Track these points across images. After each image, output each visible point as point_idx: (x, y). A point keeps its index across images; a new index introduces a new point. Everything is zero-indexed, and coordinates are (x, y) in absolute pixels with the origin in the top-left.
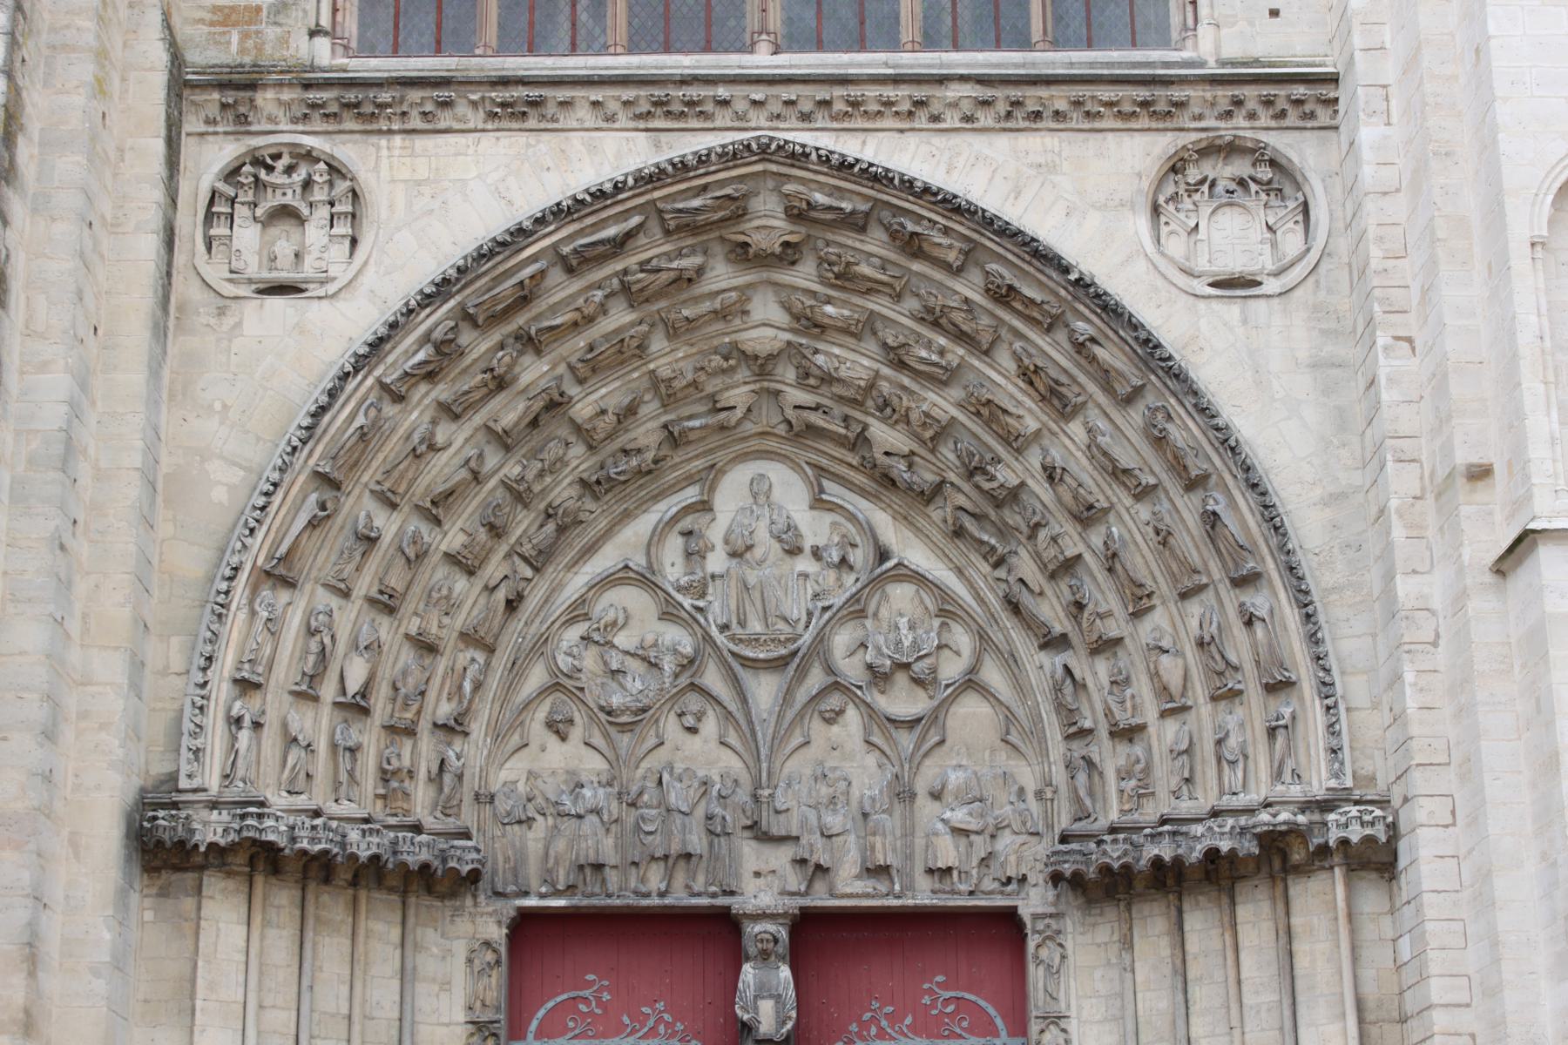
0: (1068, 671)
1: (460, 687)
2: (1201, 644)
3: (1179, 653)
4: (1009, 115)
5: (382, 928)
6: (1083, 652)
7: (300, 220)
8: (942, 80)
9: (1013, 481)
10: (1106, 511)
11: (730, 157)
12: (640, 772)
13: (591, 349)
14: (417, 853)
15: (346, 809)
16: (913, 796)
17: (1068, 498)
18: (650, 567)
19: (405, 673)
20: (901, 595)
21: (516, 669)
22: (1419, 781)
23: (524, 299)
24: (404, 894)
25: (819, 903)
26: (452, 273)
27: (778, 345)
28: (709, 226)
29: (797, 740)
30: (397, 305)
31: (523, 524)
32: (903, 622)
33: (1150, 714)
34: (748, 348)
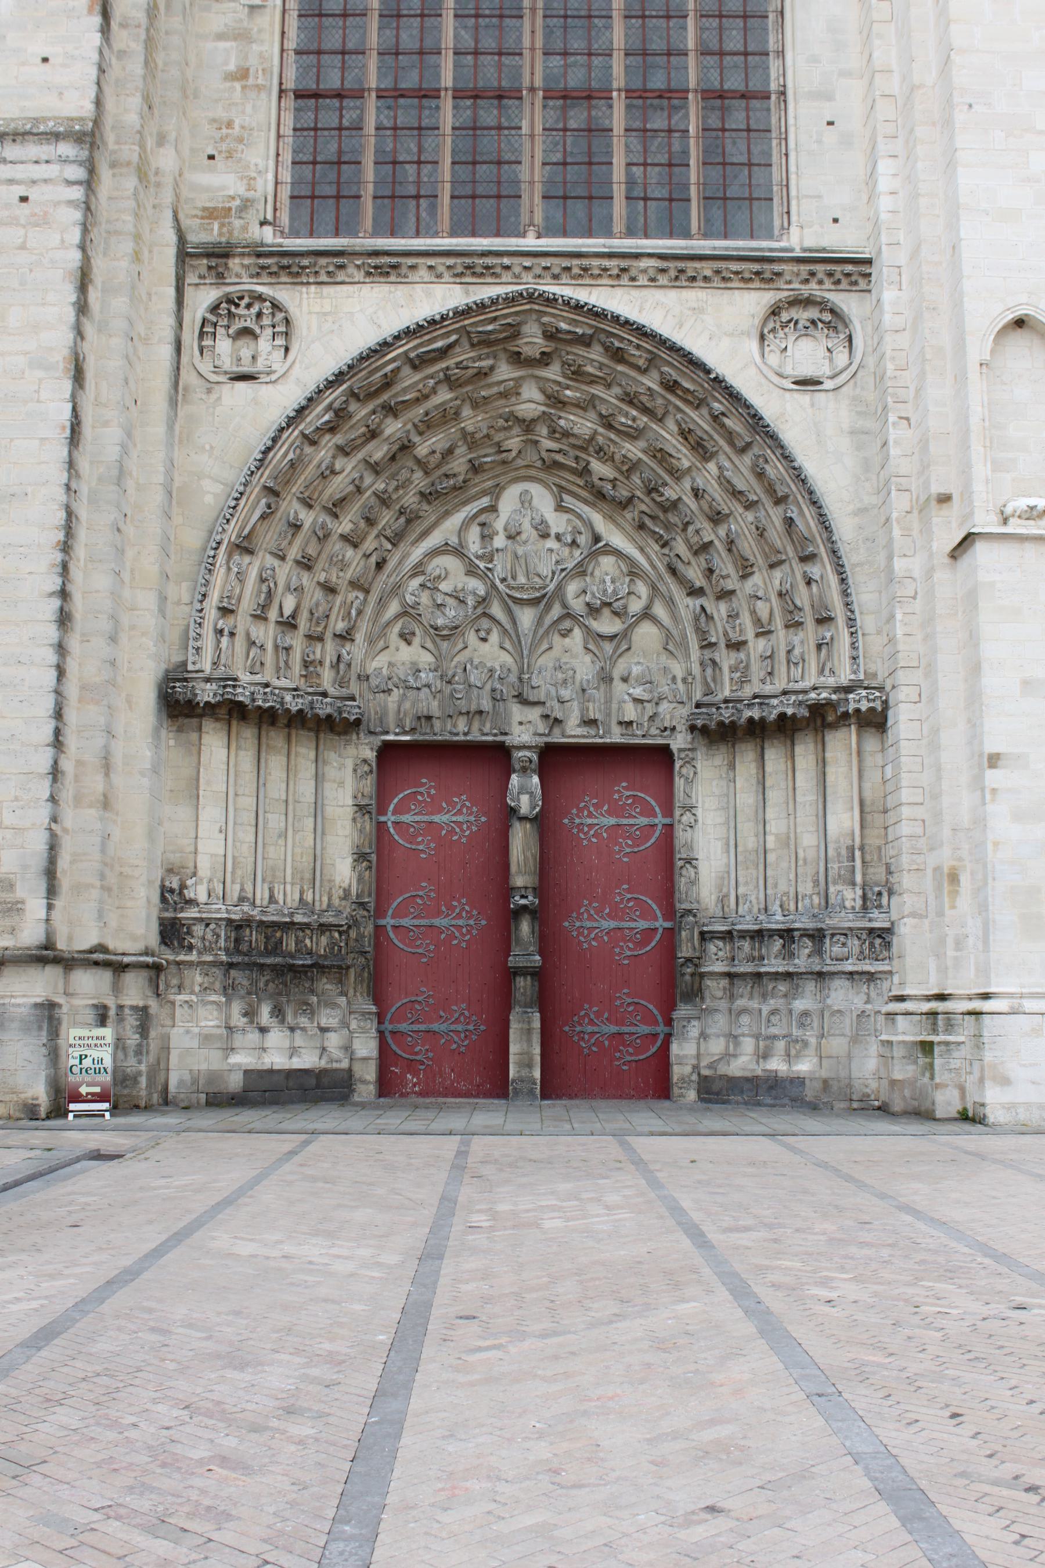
0: (703, 608)
1: (349, 613)
2: (780, 595)
3: (768, 600)
4: (677, 278)
5: (305, 752)
6: (712, 598)
7: (255, 337)
8: (637, 256)
9: (675, 497)
10: (728, 516)
11: (510, 300)
12: (454, 663)
13: (427, 414)
14: (324, 708)
15: (284, 683)
16: (611, 680)
17: (706, 507)
18: (460, 544)
19: (317, 605)
20: (607, 563)
21: (382, 603)
22: (901, 677)
23: (388, 383)
24: (317, 732)
25: (556, 740)
26: (345, 368)
27: (537, 413)
28: (498, 341)
29: (545, 646)
30: (313, 387)
31: (386, 518)
32: (608, 579)
33: (750, 634)
34: (520, 415)
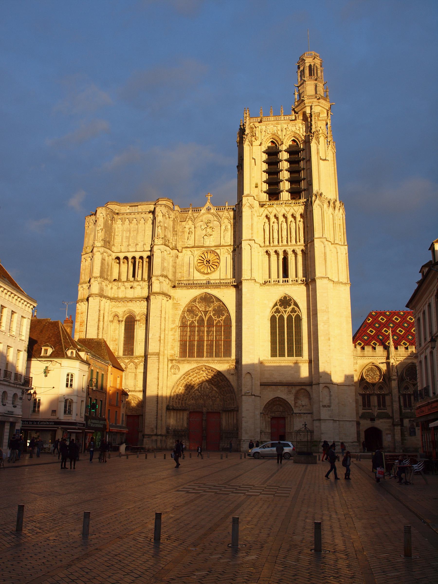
5: (182, 413)
11: (202, 366)
20: (214, 391)
21: (190, 396)
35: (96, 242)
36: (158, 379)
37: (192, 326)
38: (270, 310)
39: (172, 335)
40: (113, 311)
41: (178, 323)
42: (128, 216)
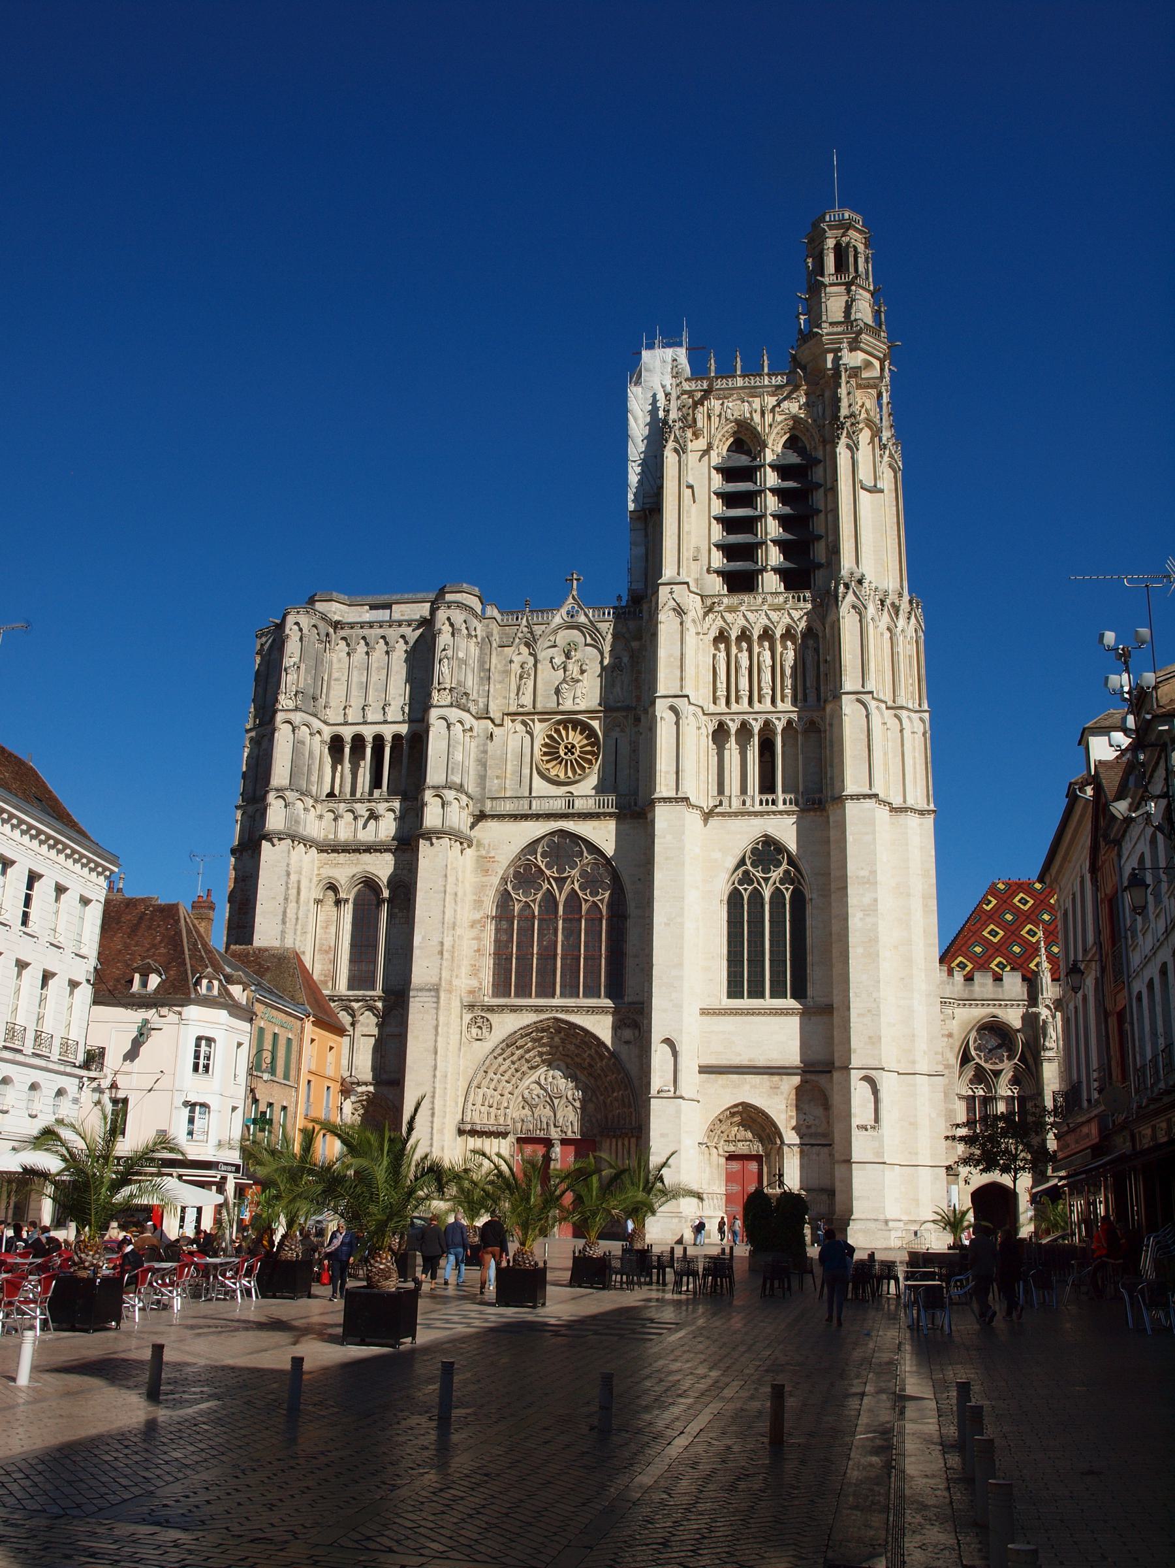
11: (548, 1019)
21: (517, 1097)
35: (281, 697)
36: (436, 1053)
37: (527, 918)
38: (727, 876)
39: (473, 939)
40: (324, 876)
41: (490, 908)
42: (366, 632)
